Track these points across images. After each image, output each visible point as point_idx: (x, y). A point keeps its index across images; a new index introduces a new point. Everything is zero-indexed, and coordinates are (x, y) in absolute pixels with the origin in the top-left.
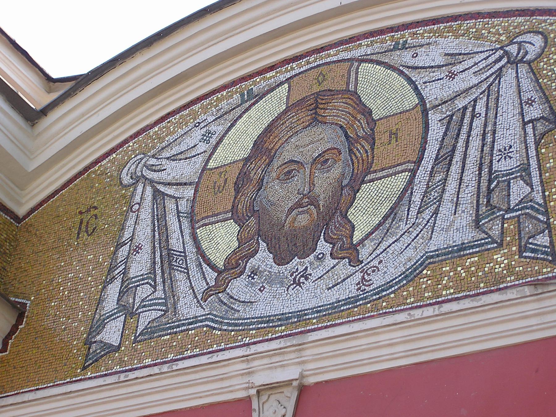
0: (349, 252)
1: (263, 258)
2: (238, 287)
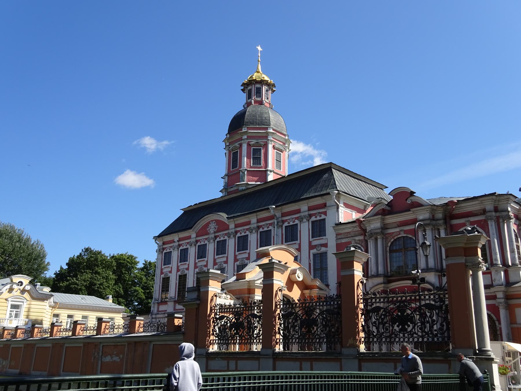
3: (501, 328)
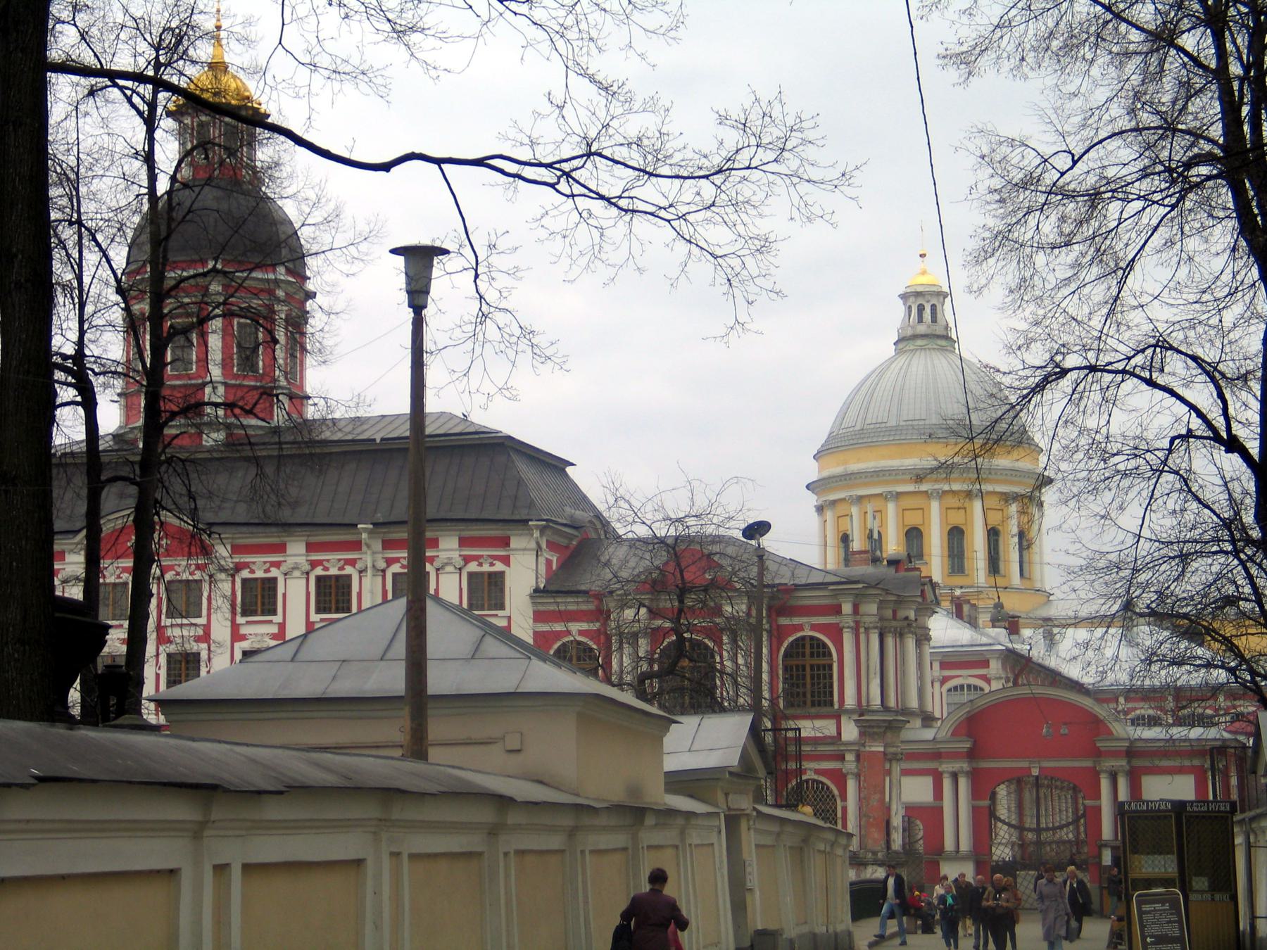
3: (844, 809)
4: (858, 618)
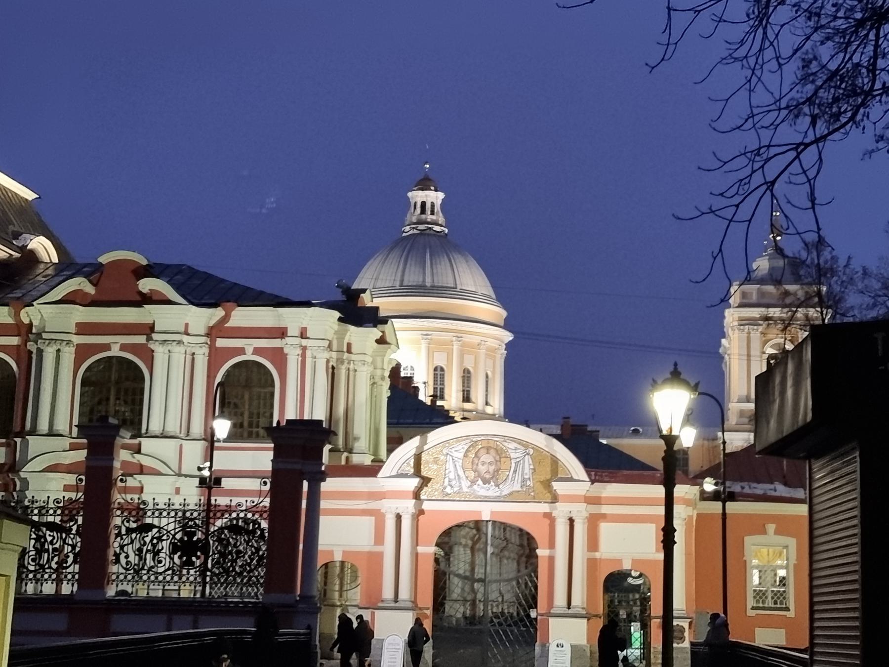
0: (497, 486)
1: (480, 482)
2: (475, 487)
4: (304, 342)
